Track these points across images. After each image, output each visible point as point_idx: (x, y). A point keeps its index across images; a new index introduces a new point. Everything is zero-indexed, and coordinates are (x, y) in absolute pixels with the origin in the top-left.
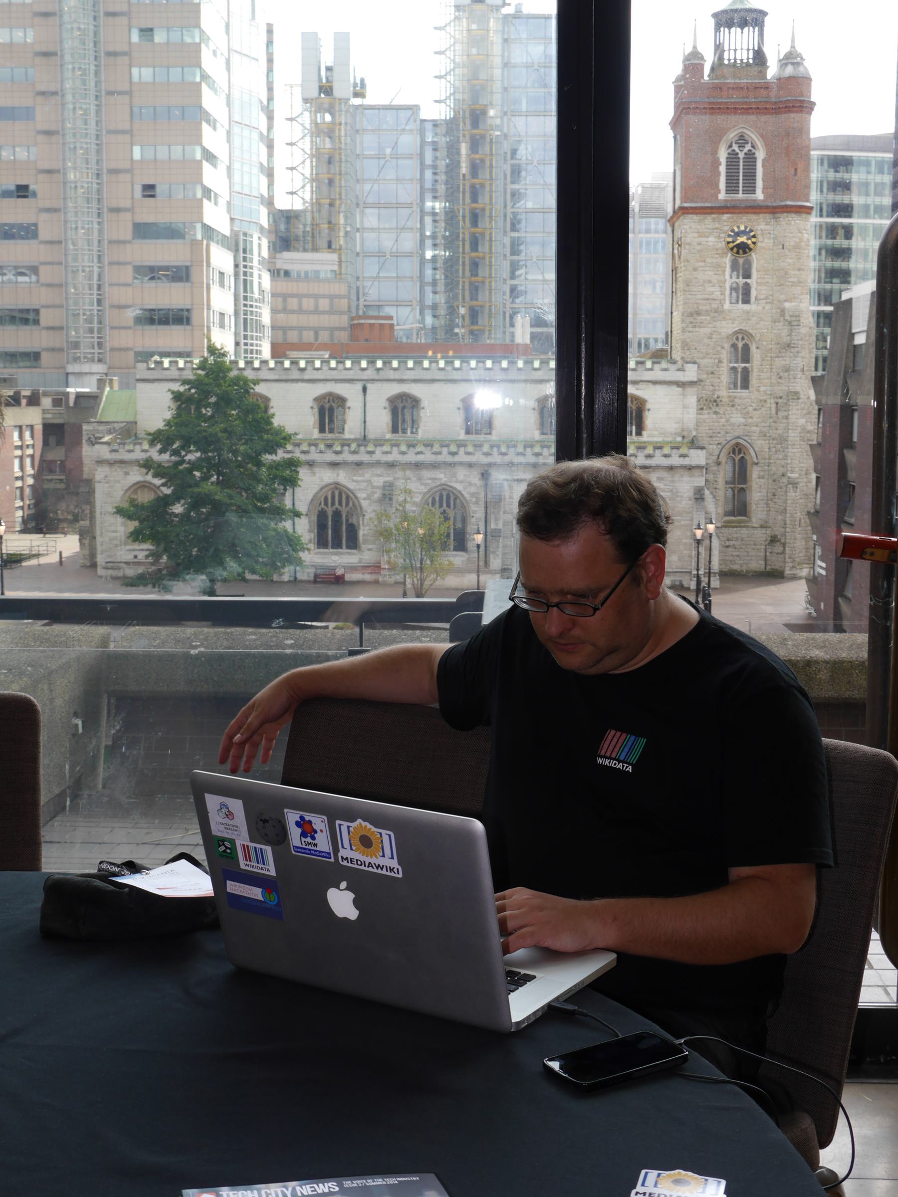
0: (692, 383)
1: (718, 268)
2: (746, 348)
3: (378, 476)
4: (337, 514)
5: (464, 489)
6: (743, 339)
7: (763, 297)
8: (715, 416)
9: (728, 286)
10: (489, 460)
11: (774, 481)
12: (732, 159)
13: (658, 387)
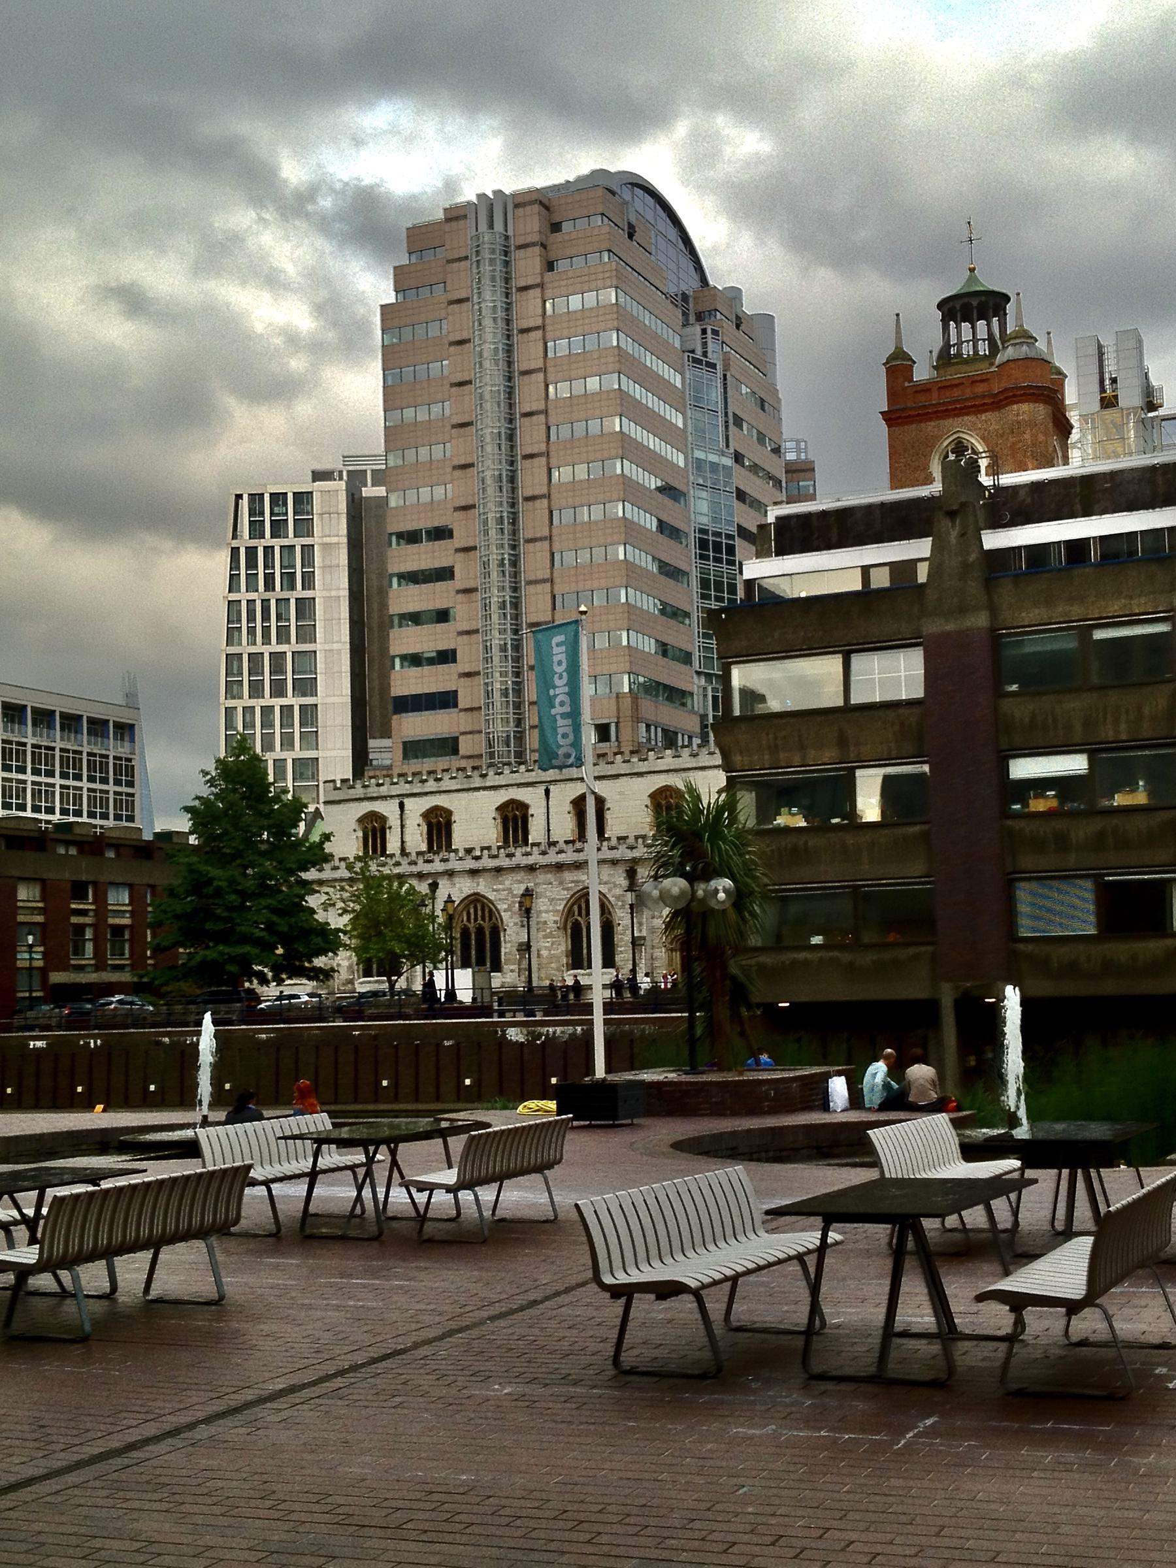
3: (520, 882)
4: (480, 931)
5: (610, 890)
10: (636, 854)
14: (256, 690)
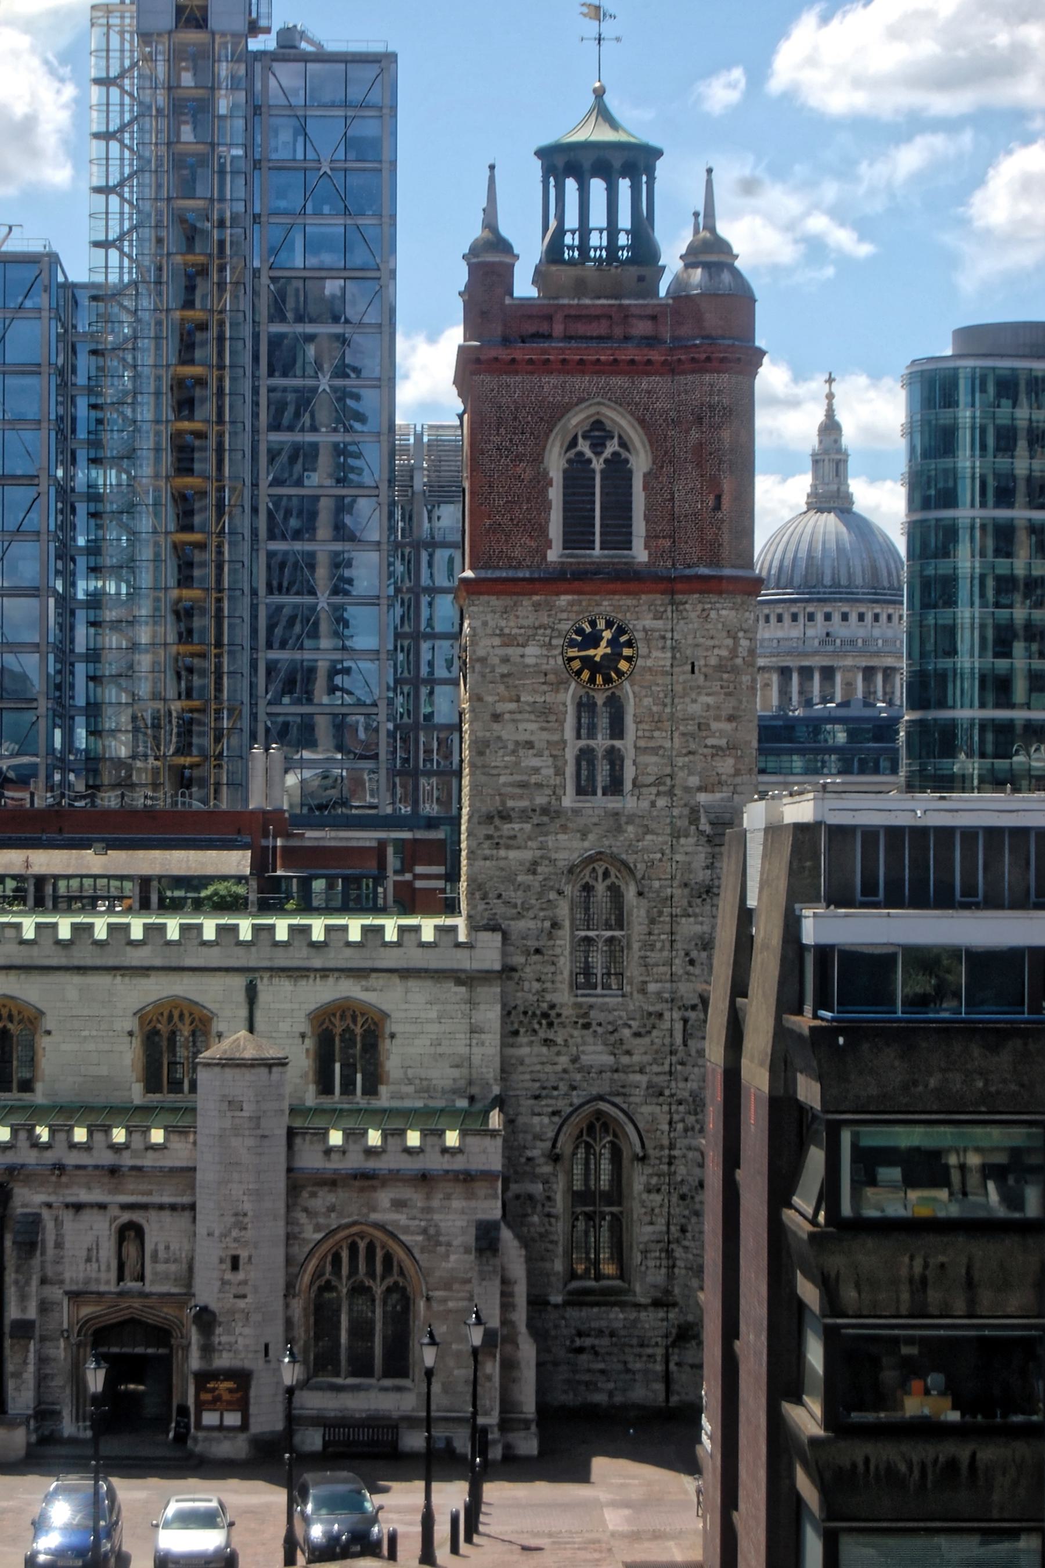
0: (485, 977)
6: (606, 874)
7: (651, 779)
8: (544, 1050)
9: (570, 754)
11: (683, 1197)
12: (577, 475)
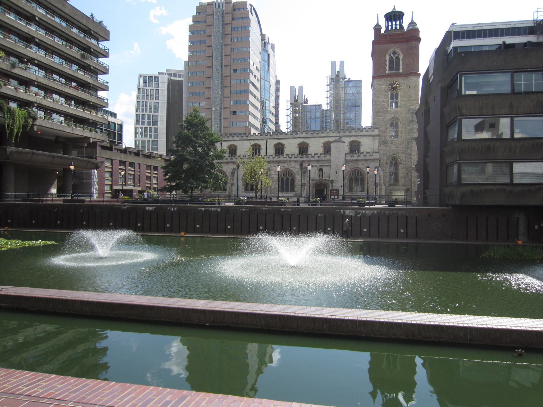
1: (386, 96)
2: (397, 124)
9: (389, 102)
10: (302, 159)
12: (391, 60)
13: (365, 137)
14: (143, 123)
